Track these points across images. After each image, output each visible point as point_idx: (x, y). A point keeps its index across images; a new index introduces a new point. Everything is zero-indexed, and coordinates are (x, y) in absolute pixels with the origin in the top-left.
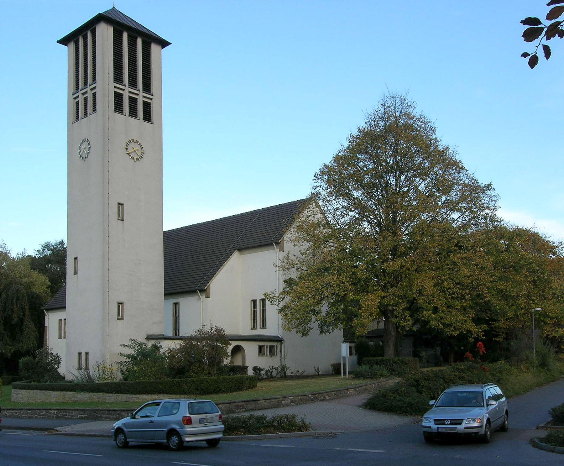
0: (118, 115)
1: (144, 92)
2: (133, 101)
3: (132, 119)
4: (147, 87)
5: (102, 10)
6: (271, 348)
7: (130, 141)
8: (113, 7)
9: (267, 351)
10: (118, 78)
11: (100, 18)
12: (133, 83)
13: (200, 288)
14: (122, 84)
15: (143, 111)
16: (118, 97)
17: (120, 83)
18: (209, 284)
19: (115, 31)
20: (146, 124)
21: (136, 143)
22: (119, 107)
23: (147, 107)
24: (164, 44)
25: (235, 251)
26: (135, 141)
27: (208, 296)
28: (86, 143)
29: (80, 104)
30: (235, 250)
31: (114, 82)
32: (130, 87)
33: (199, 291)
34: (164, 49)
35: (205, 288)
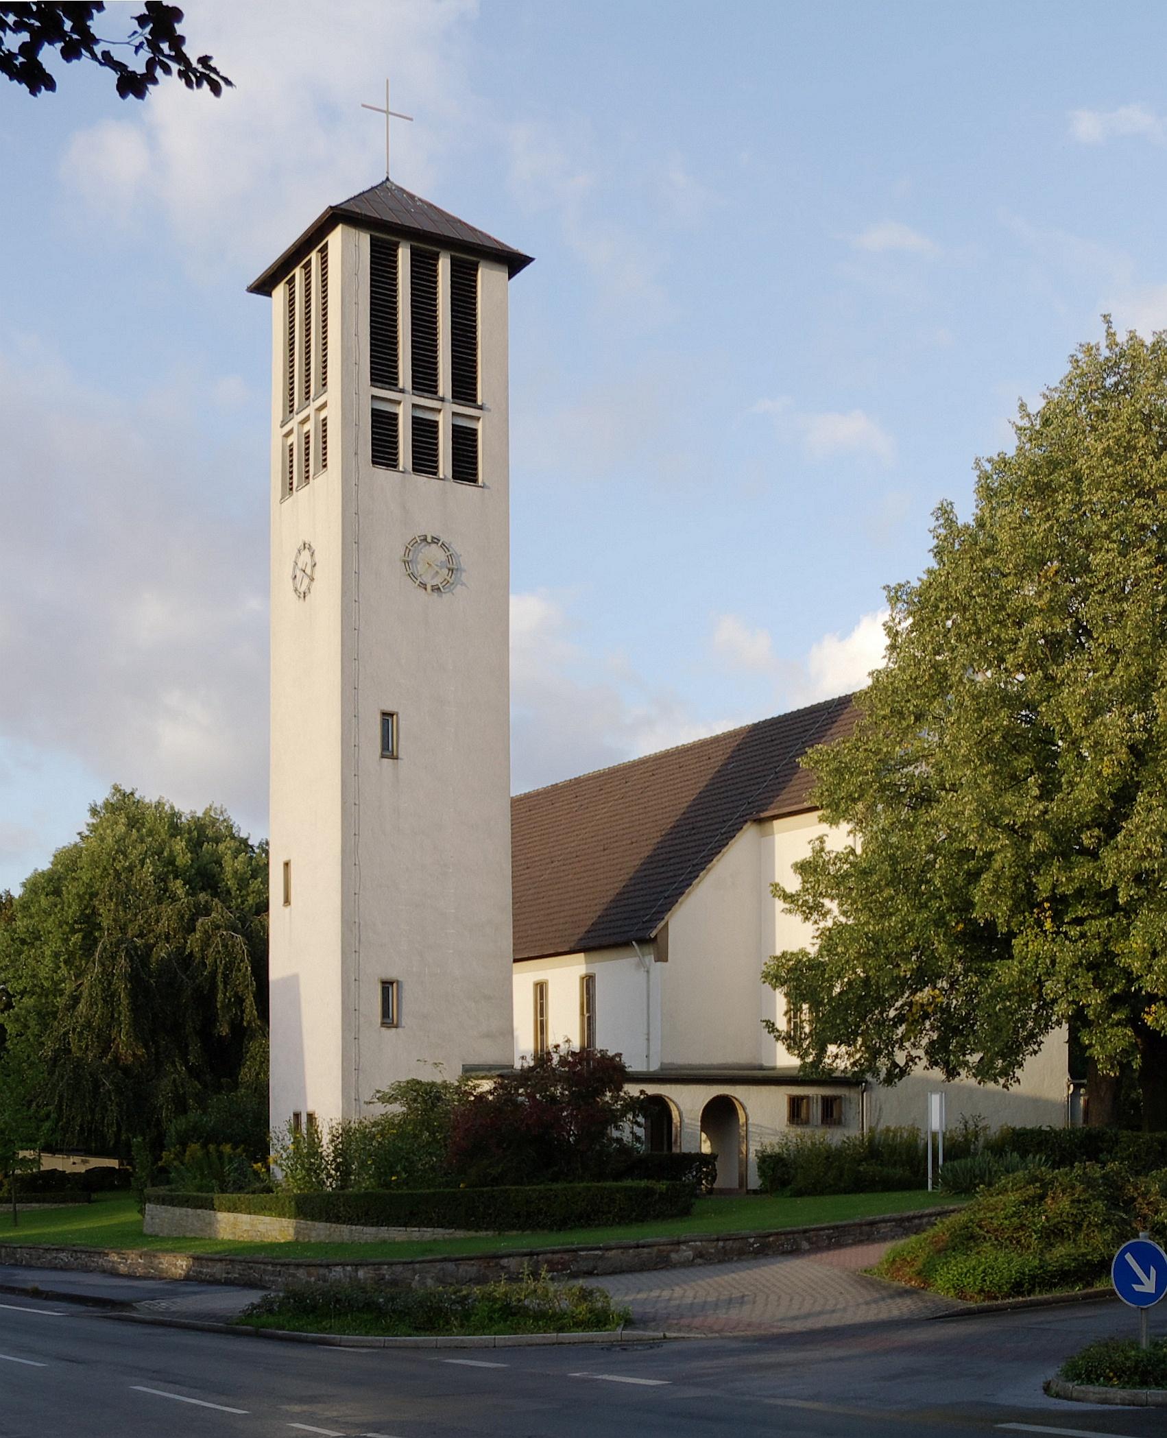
0: (382, 473)
1: (456, 401)
2: (424, 431)
3: (422, 480)
4: (465, 388)
5: (338, 198)
6: (828, 1103)
7: (414, 542)
8: (384, 179)
9: (816, 1111)
10: (383, 372)
11: (335, 217)
12: (425, 380)
13: (640, 934)
14: (393, 387)
15: (454, 454)
16: (383, 424)
17: (387, 386)
18: (663, 923)
19: (375, 245)
20: (464, 489)
21: (433, 546)
22: (384, 453)
23: (465, 440)
24: (515, 262)
25: (745, 827)
26: (429, 540)
27: (662, 957)
28: (306, 553)
29: (312, 439)
30: (746, 822)
31: (372, 385)
32: (415, 392)
33: (636, 942)
34: (518, 275)
35: (652, 935)
